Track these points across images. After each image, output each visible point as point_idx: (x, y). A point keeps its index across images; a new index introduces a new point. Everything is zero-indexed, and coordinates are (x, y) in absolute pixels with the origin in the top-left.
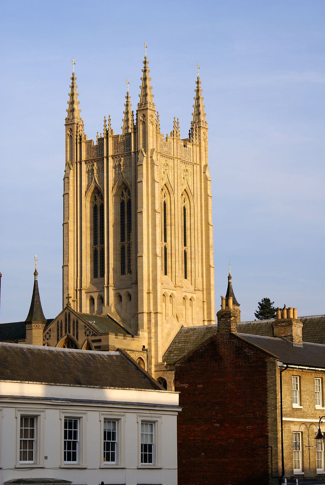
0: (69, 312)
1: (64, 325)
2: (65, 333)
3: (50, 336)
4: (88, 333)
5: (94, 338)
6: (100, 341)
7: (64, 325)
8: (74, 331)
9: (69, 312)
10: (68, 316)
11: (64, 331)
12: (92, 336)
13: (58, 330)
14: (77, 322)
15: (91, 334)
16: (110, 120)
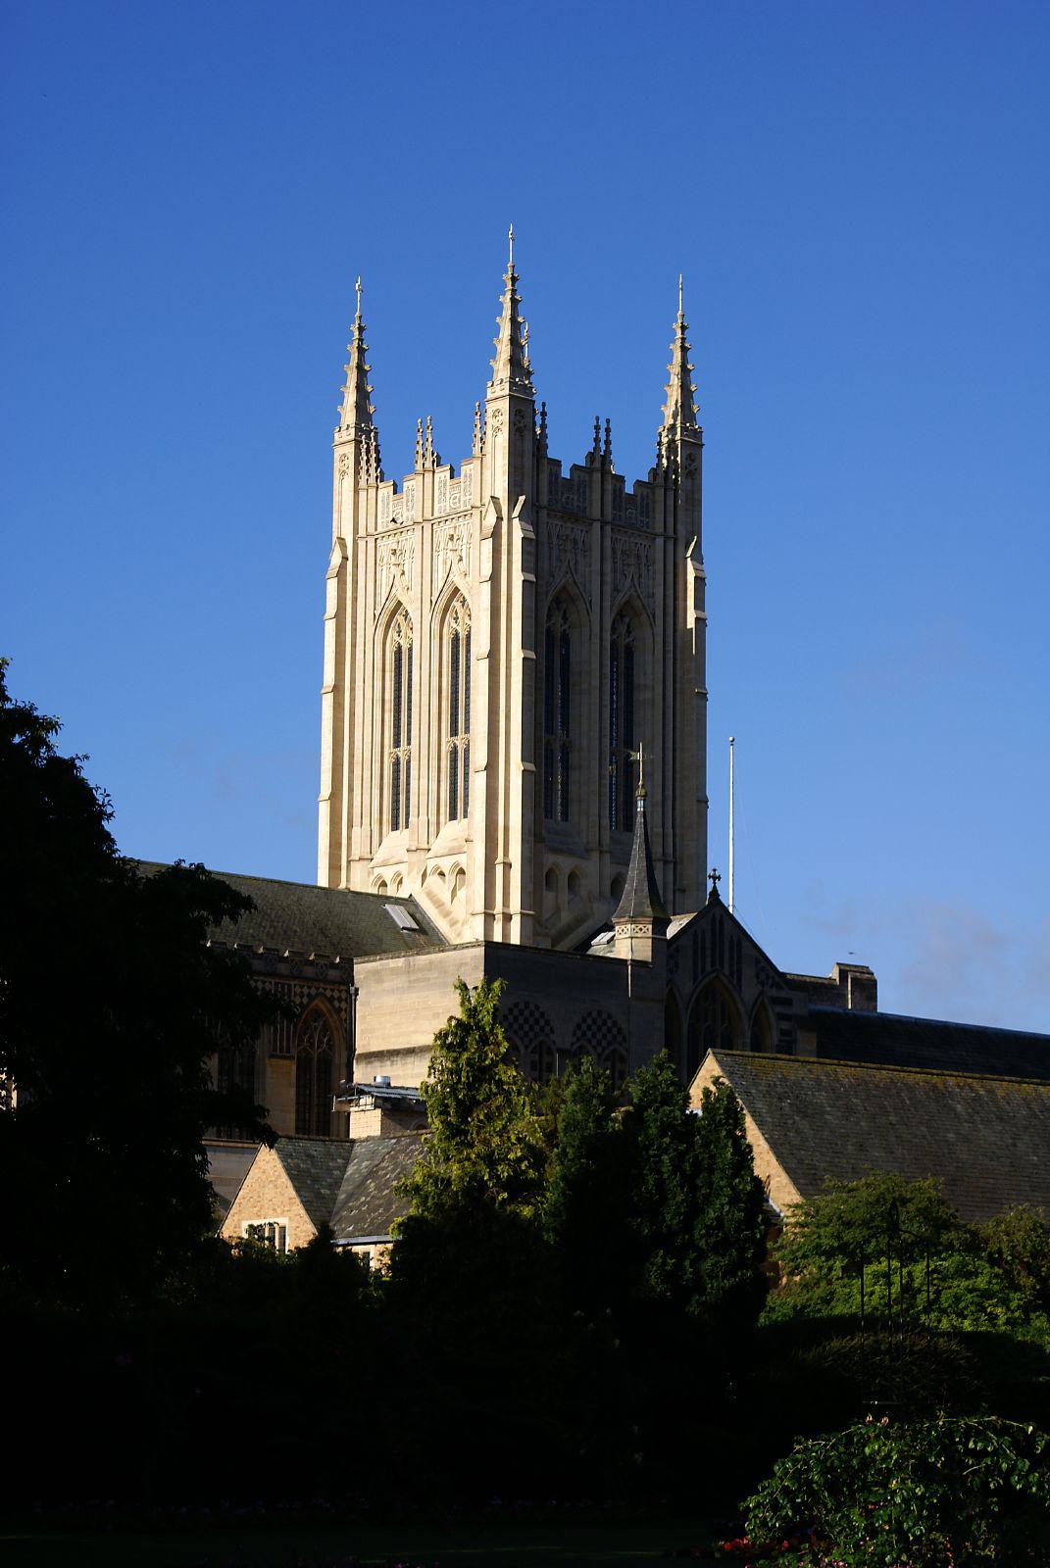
0: (722, 916)
1: (708, 945)
2: (712, 966)
3: (677, 965)
4: (763, 976)
5: (774, 992)
6: (788, 1002)
7: (708, 945)
8: (731, 966)
9: (722, 916)
10: (718, 924)
11: (708, 960)
12: (772, 986)
13: (695, 953)
14: (739, 943)
15: (770, 982)
16: (608, 430)
